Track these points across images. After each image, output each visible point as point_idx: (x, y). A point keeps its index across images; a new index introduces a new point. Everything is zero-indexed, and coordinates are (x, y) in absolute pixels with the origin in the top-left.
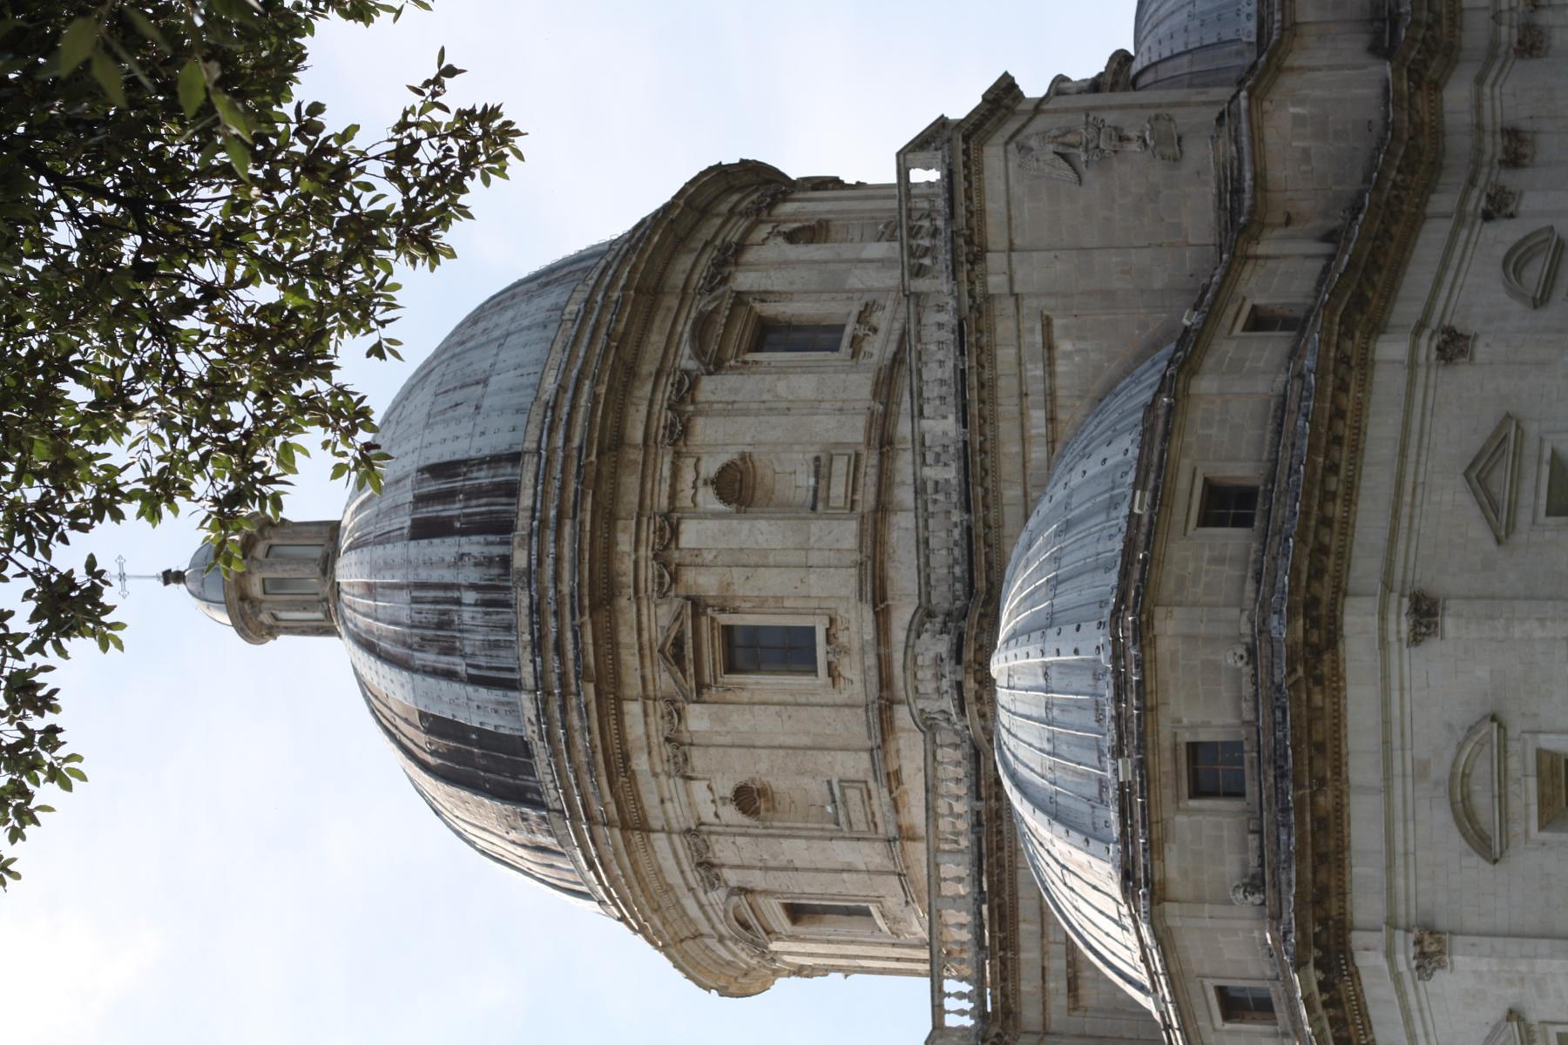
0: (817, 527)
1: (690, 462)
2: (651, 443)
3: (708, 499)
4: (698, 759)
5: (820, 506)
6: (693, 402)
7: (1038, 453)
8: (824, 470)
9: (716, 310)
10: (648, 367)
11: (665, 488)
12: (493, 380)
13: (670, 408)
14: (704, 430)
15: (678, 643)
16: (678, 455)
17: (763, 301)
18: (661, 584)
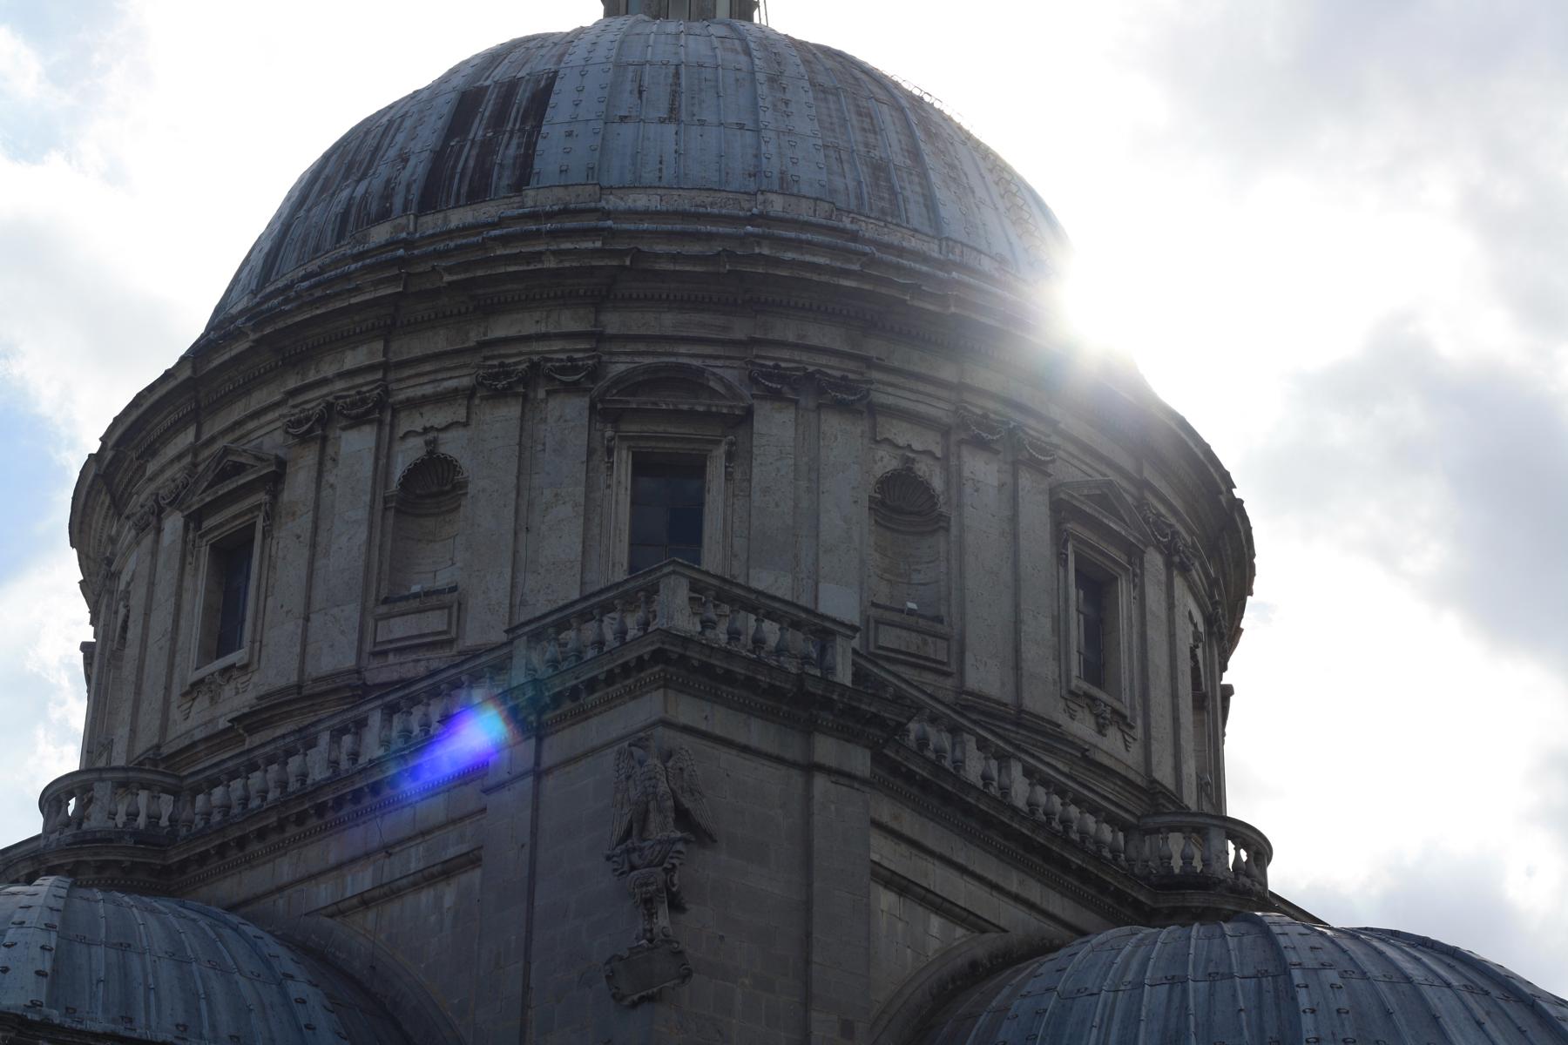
0: (352, 611)
1: (460, 414)
2: (487, 352)
3: (408, 454)
4: (148, 541)
5: (383, 609)
6: (548, 393)
7: (324, 893)
8: (434, 601)
9: (713, 393)
10: (613, 322)
11: (428, 390)
12: (672, 128)
13: (534, 366)
14: (501, 419)
15: (239, 469)
16: (470, 394)
17: (730, 456)
18: (299, 423)
